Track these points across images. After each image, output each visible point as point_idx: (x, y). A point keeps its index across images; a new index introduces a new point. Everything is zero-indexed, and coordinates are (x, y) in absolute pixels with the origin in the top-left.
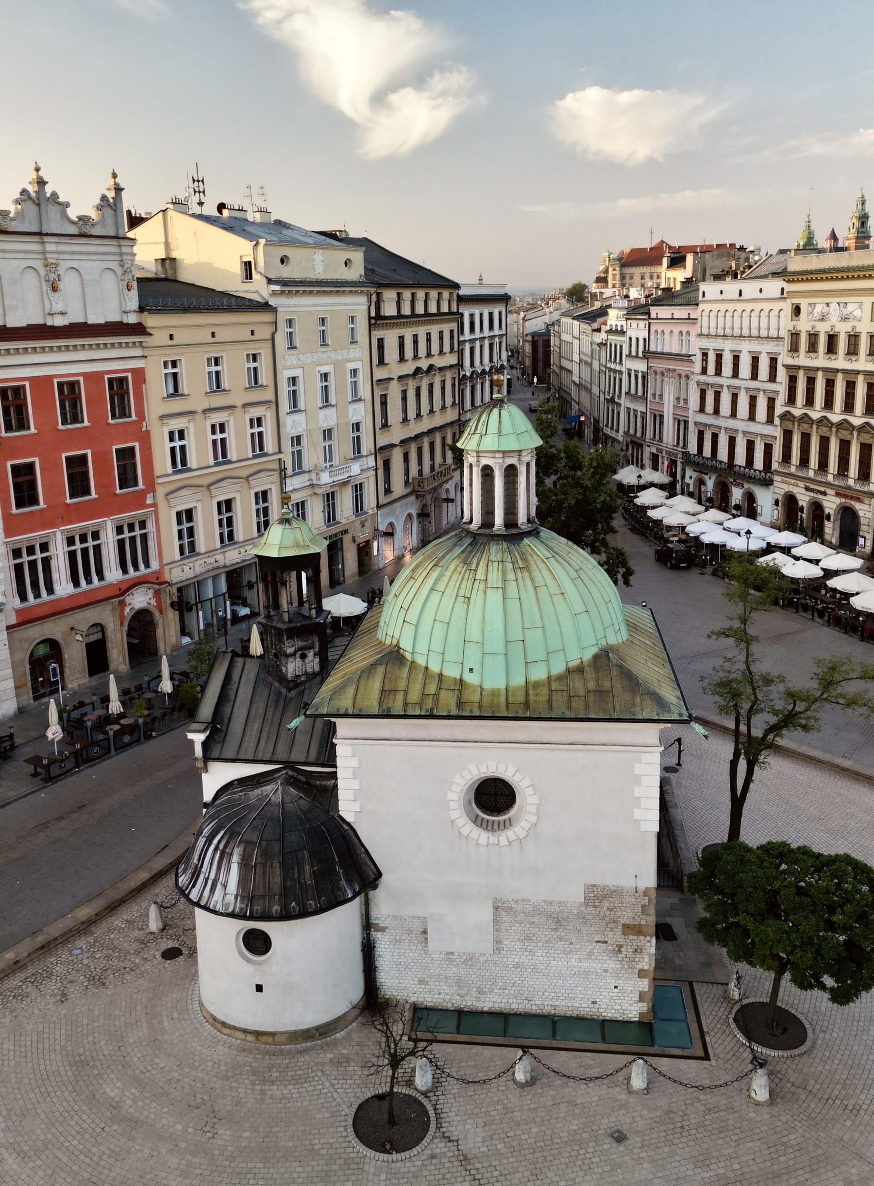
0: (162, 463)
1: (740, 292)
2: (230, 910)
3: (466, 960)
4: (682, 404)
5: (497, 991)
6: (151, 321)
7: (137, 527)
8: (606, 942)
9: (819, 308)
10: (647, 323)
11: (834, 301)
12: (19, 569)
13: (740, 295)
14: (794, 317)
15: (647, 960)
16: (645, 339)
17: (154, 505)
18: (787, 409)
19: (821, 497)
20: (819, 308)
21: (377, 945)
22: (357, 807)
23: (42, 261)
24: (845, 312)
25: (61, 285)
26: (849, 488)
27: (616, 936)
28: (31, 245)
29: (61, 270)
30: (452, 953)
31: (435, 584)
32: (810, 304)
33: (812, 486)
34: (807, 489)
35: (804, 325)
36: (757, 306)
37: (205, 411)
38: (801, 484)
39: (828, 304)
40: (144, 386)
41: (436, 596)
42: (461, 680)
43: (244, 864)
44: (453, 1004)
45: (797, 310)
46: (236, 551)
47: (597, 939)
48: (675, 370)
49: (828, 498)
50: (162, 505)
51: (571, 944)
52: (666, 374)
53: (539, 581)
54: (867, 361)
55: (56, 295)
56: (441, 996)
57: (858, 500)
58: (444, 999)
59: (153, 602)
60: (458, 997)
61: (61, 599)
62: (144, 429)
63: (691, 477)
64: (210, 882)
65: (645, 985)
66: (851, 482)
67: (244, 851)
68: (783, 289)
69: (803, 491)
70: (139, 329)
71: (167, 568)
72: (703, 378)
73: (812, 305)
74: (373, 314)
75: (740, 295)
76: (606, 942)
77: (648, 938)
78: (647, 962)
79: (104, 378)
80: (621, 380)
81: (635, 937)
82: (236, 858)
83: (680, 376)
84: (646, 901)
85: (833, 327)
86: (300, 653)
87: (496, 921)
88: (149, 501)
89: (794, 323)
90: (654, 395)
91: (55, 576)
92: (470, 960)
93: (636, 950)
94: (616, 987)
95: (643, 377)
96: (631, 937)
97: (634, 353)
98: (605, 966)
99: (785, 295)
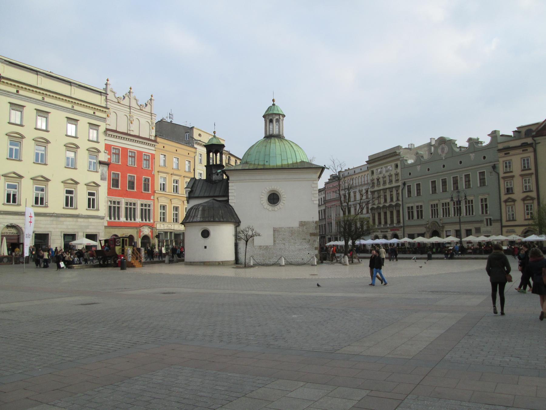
0: (157, 188)
1: (355, 171)
2: (199, 220)
3: (265, 248)
4: (338, 215)
5: (274, 258)
6: (159, 140)
7: (148, 206)
9: (379, 170)
10: (324, 191)
11: (383, 166)
12: (110, 207)
15: (317, 244)
16: (324, 197)
17: (153, 200)
19: (386, 233)
20: (379, 170)
21: (239, 245)
24: (387, 169)
26: (394, 227)
27: (308, 237)
30: (261, 246)
32: (376, 169)
33: (383, 230)
34: (382, 232)
35: (375, 176)
36: (360, 175)
37: (171, 174)
38: (379, 231)
39: (382, 168)
40: (154, 160)
41: (257, 147)
42: (264, 164)
44: (261, 263)
45: (373, 173)
46: (178, 226)
47: (303, 238)
48: (335, 205)
49: (389, 233)
50: (156, 200)
51: (296, 240)
52: (332, 207)
53: (285, 143)
54: (395, 183)
56: (258, 261)
57: (398, 230)
58: (259, 262)
59: (150, 233)
60: (263, 261)
61: (121, 222)
62: (153, 174)
65: (317, 252)
66: (395, 225)
67: (203, 208)
68: (368, 167)
69: (380, 233)
70: (155, 141)
71: (156, 223)
73: (377, 170)
74: (227, 162)
76: (305, 239)
77: (317, 237)
78: (317, 245)
81: (313, 237)
83: (337, 206)
84: (316, 225)
85: (384, 175)
87: (274, 235)
88: (152, 198)
89: (372, 177)
90: (328, 216)
91: (121, 214)
92: (267, 248)
93: (314, 241)
94: (309, 254)
95: (324, 211)
96: (312, 237)
98: (305, 247)
99: (369, 169)
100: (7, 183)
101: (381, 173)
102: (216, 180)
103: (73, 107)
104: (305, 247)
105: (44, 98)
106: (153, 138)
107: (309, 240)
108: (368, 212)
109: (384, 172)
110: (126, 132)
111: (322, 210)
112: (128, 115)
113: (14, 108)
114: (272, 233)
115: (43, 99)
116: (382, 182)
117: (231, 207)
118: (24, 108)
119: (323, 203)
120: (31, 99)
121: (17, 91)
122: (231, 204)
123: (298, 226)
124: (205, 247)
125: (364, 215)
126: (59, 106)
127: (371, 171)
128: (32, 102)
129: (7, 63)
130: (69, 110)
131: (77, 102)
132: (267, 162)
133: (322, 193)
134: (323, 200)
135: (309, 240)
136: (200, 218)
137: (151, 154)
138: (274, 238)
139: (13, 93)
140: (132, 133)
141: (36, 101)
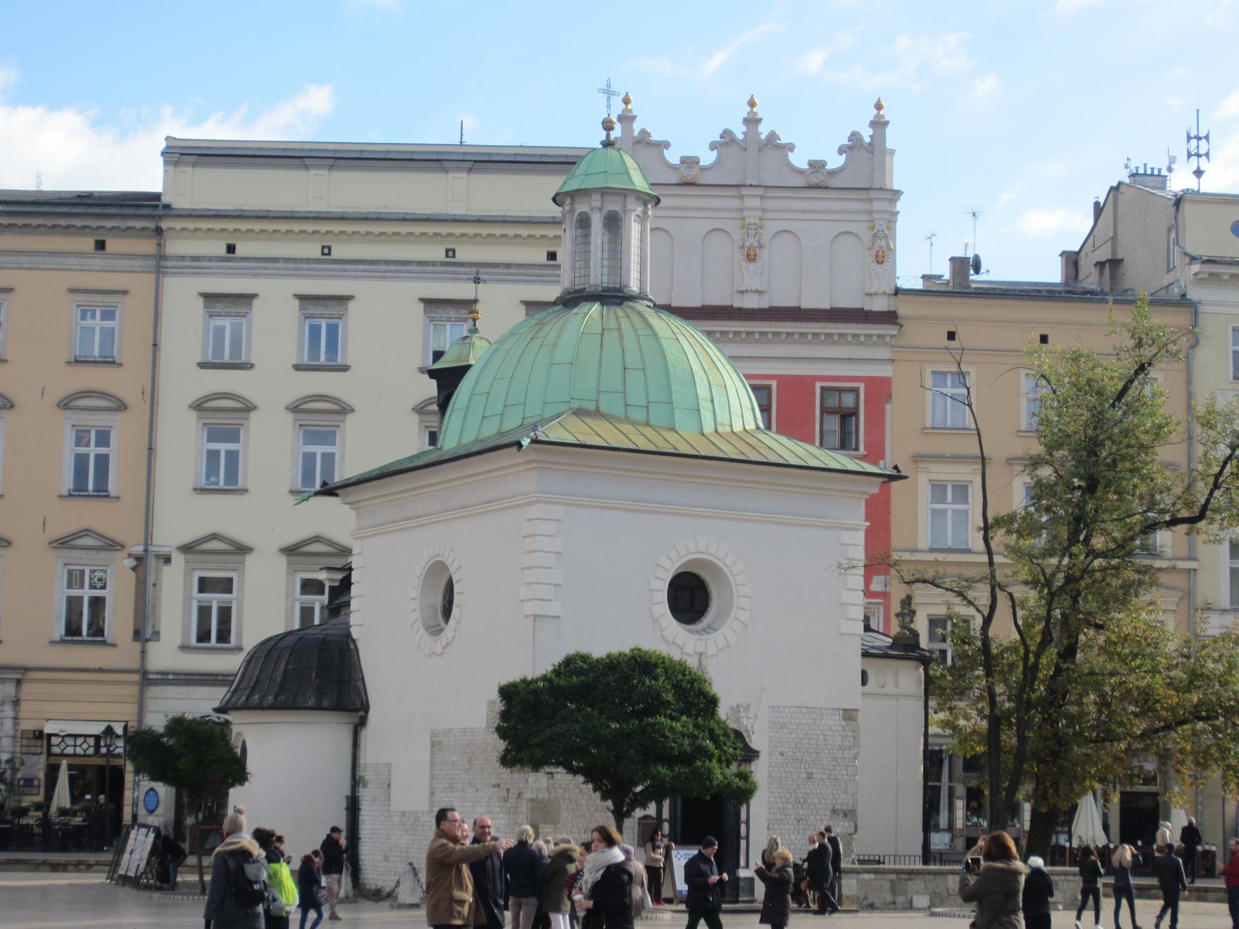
8: (499, 786)
15: (525, 811)
23: (740, 222)
25: (764, 254)
28: (727, 202)
29: (767, 234)
30: (403, 814)
47: (493, 781)
55: (752, 266)
76: (499, 786)
79: (814, 386)
87: (432, 764)
100: (196, 576)
103: (451, 254)
104: (498, 821)
105: (329, 248)
106: (879, 305)
107: (508, 790)
110: (726, 302)
112: (733, 227)
113: (219, 308)
115: (326, 251)
117: (352, 646)
118: (255, 302)
120: (279, 265)
121: (231, 249)
123: (484, 725)
126: (387, 262)
128: (279, 275)
129: (194, 159)
130: (431, 268)
131: (458, 230)
135: (508, 790)
137: (869, 381)
138: (432, 777)
139: (210, 259)
140: (751, 302)
141: (296, 265)
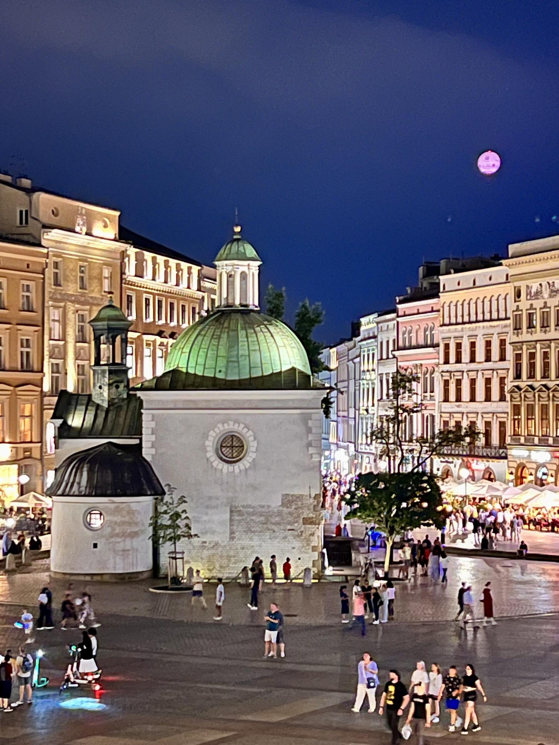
2: (83, 493)
13: (474, 284)
14: (517, 299)
18: (516, 384)
22: (153, 451)
31: (201, 331)
35: (524, 304)
41: (200, 338)
43: (90, 472)
48: (421, 365)
63: (438, 470)
64: (69, 485)
72: (447, 367)
75: (474, 284)
80: (373, 389)
82: (85, 469)
86: (115, 384)
87: (231, 520)
89: (517, 303)
94: (299, 559)
97: (384, 356)
101: (538, 294)
102: (114, 399)
108: (502, 398)
109: (546, 295)
111: (387, 374)
114: (227, 516)
116: (537, 322)
117: (146, 464)
119: (391, 356)
122: (148, 458)
124: (95, 546)
125: (495, 404)
127: (515, 287)
132: (220, 371)
133: (390, 327)
134: (391, 348)
136: (86, 488)
